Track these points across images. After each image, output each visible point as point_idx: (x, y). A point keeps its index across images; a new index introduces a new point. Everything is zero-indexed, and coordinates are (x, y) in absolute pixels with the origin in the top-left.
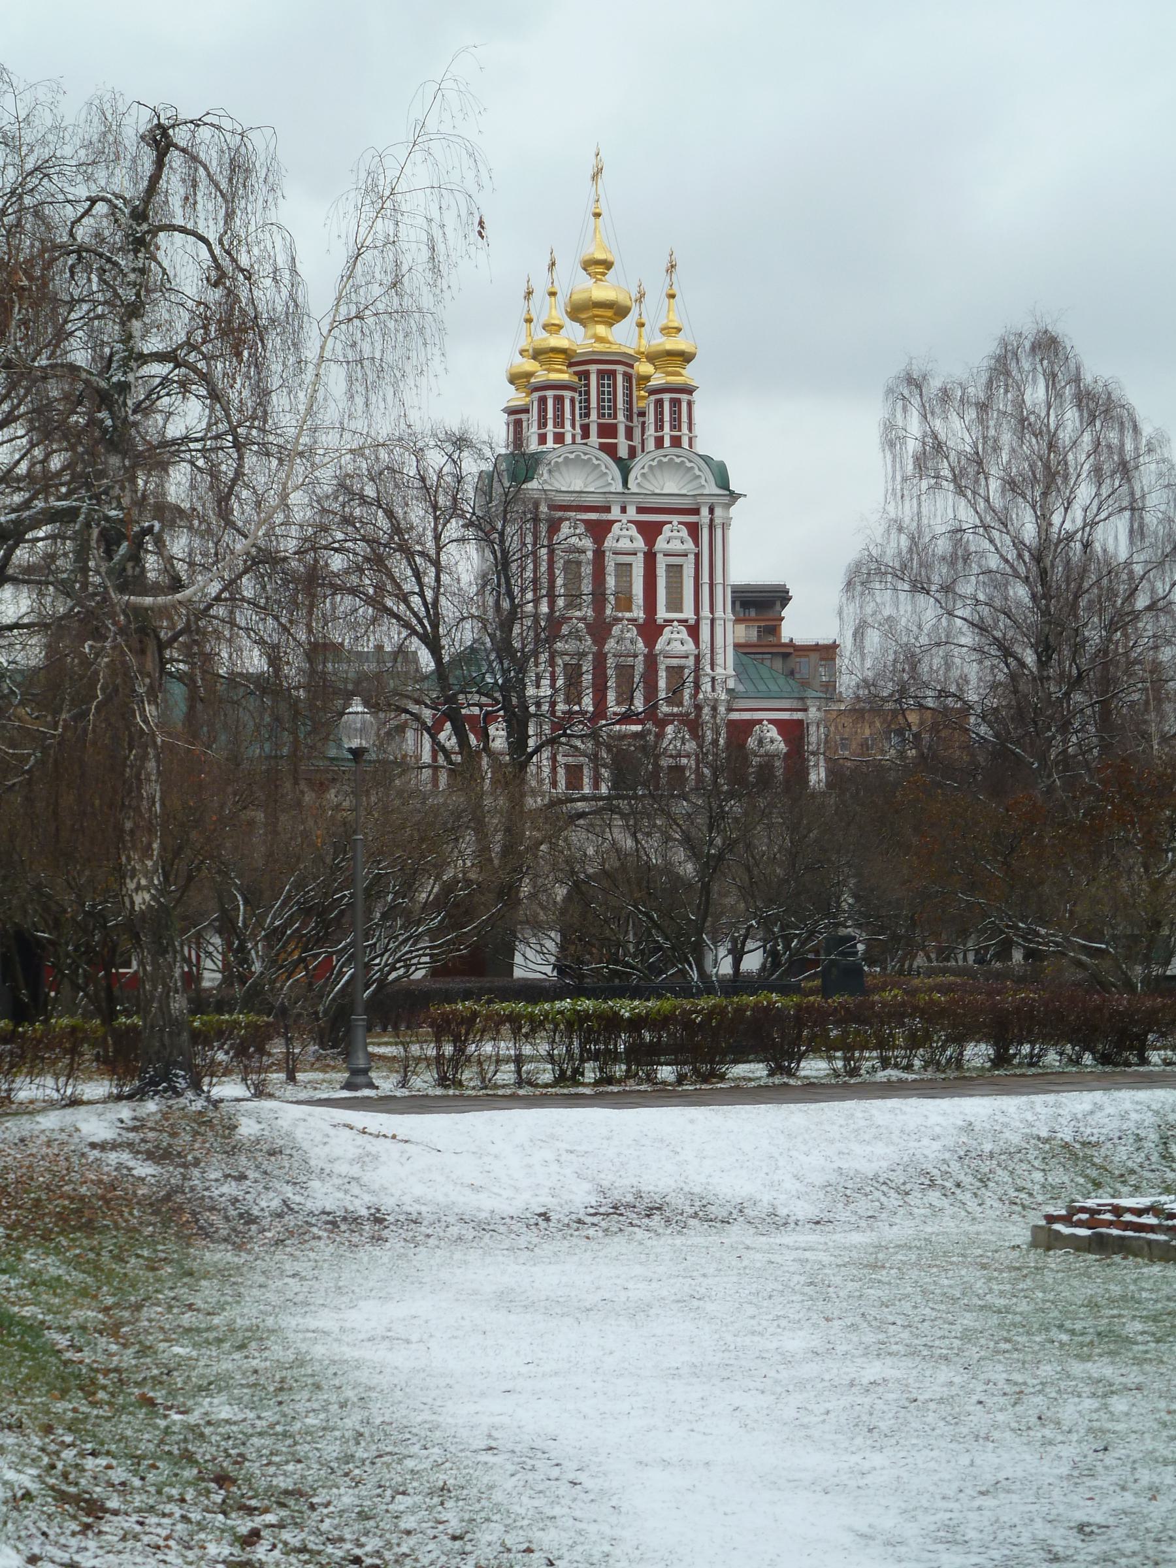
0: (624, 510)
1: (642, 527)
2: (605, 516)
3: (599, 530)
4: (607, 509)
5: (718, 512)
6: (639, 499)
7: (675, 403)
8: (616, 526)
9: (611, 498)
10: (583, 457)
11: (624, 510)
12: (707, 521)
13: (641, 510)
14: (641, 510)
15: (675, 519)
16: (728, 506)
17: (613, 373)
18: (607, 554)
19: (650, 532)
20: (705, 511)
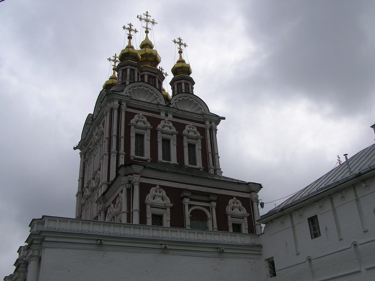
0: (167, 115)
1: (174, 124)
2: (156, 116)
3: (154, 122)
4: (159, 114)
6: (175, 110)
7: (186, 84)
8: (162, 123)
9: (161, 107)
10: (145, 89)
11: (167, 115)
14: (174, 117)
15: (191, 124)
17: (155, 78)
18: (159, 132)
19: (180, 127)
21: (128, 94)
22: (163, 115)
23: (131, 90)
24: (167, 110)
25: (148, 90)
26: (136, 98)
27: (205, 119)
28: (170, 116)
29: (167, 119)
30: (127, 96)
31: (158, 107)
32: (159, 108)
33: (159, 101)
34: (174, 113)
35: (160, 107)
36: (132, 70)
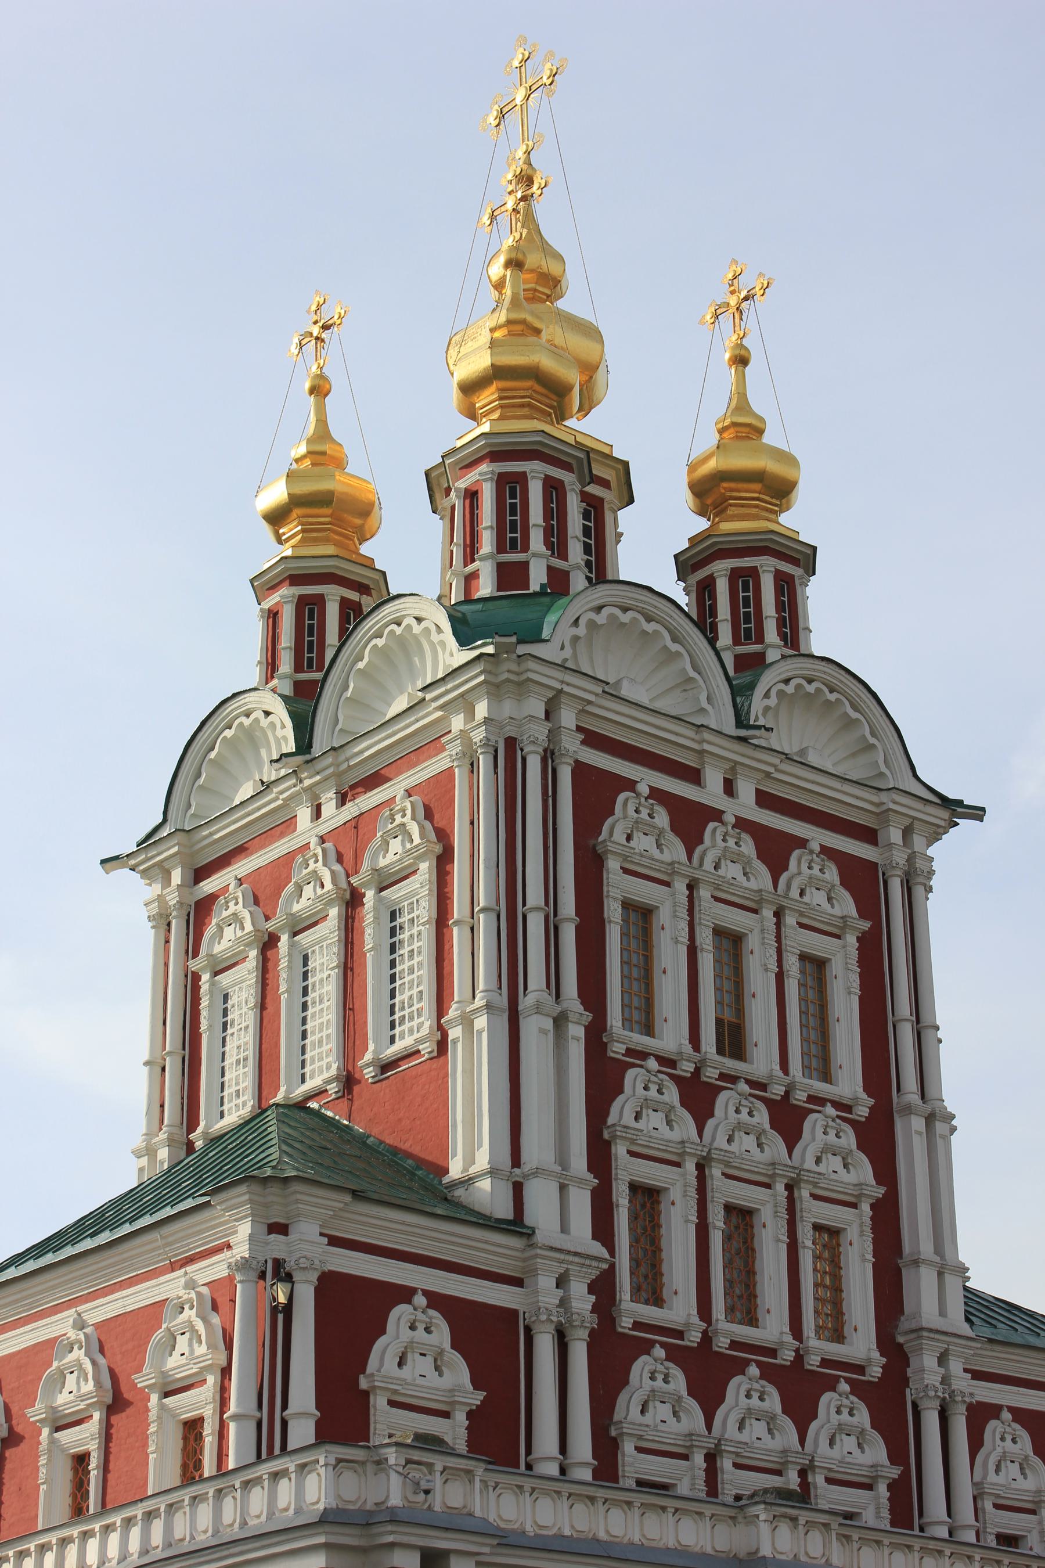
0: (729, 788)
4: (694, 776)
5: (918, 842)
11: (729, 788)
12: (900, 857)
13: (764, 799)
14: (764, 799)
16: (935, 835)
20: (896, 835)
21: (568, 653)
22: (714, 779)
23: (581, 631)
24: (736, 763)
25: (656, 632)
26: (593, 668)
27: (884, 815)
28: (746, 791)
29: (730, 819)
30: (562, 666)
31: (700, 742)
32: (706, 747)
33: (704, 704)
34: (768, 775)
35: (709, 743)
36: (553, 489)
